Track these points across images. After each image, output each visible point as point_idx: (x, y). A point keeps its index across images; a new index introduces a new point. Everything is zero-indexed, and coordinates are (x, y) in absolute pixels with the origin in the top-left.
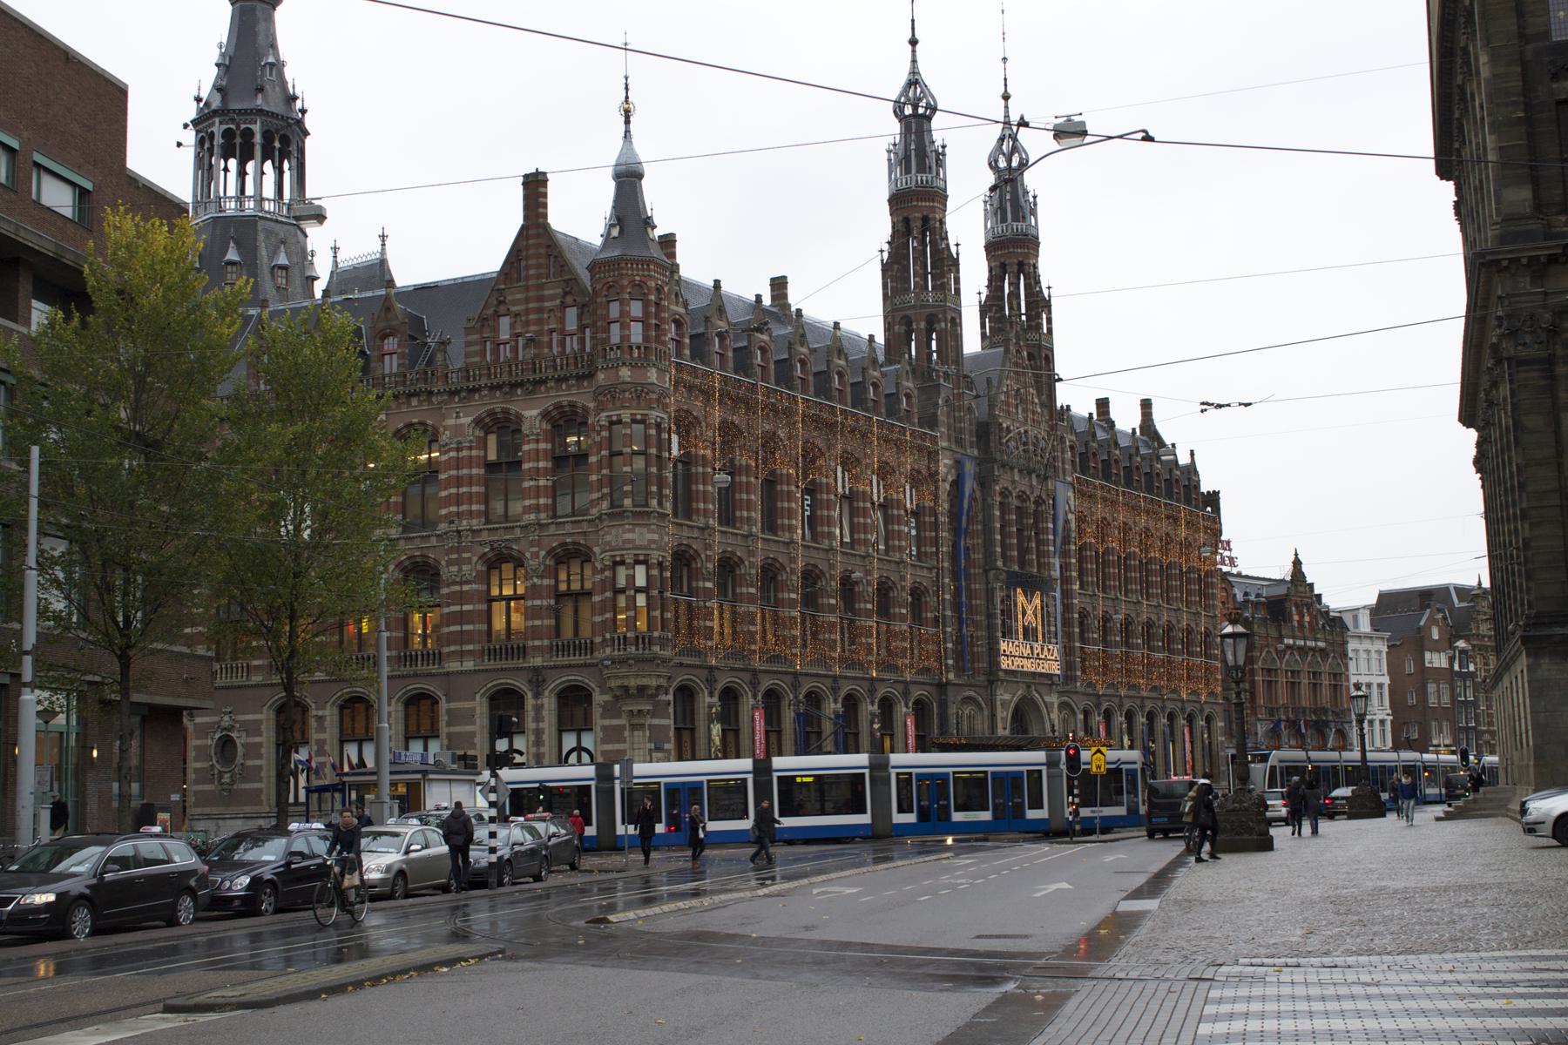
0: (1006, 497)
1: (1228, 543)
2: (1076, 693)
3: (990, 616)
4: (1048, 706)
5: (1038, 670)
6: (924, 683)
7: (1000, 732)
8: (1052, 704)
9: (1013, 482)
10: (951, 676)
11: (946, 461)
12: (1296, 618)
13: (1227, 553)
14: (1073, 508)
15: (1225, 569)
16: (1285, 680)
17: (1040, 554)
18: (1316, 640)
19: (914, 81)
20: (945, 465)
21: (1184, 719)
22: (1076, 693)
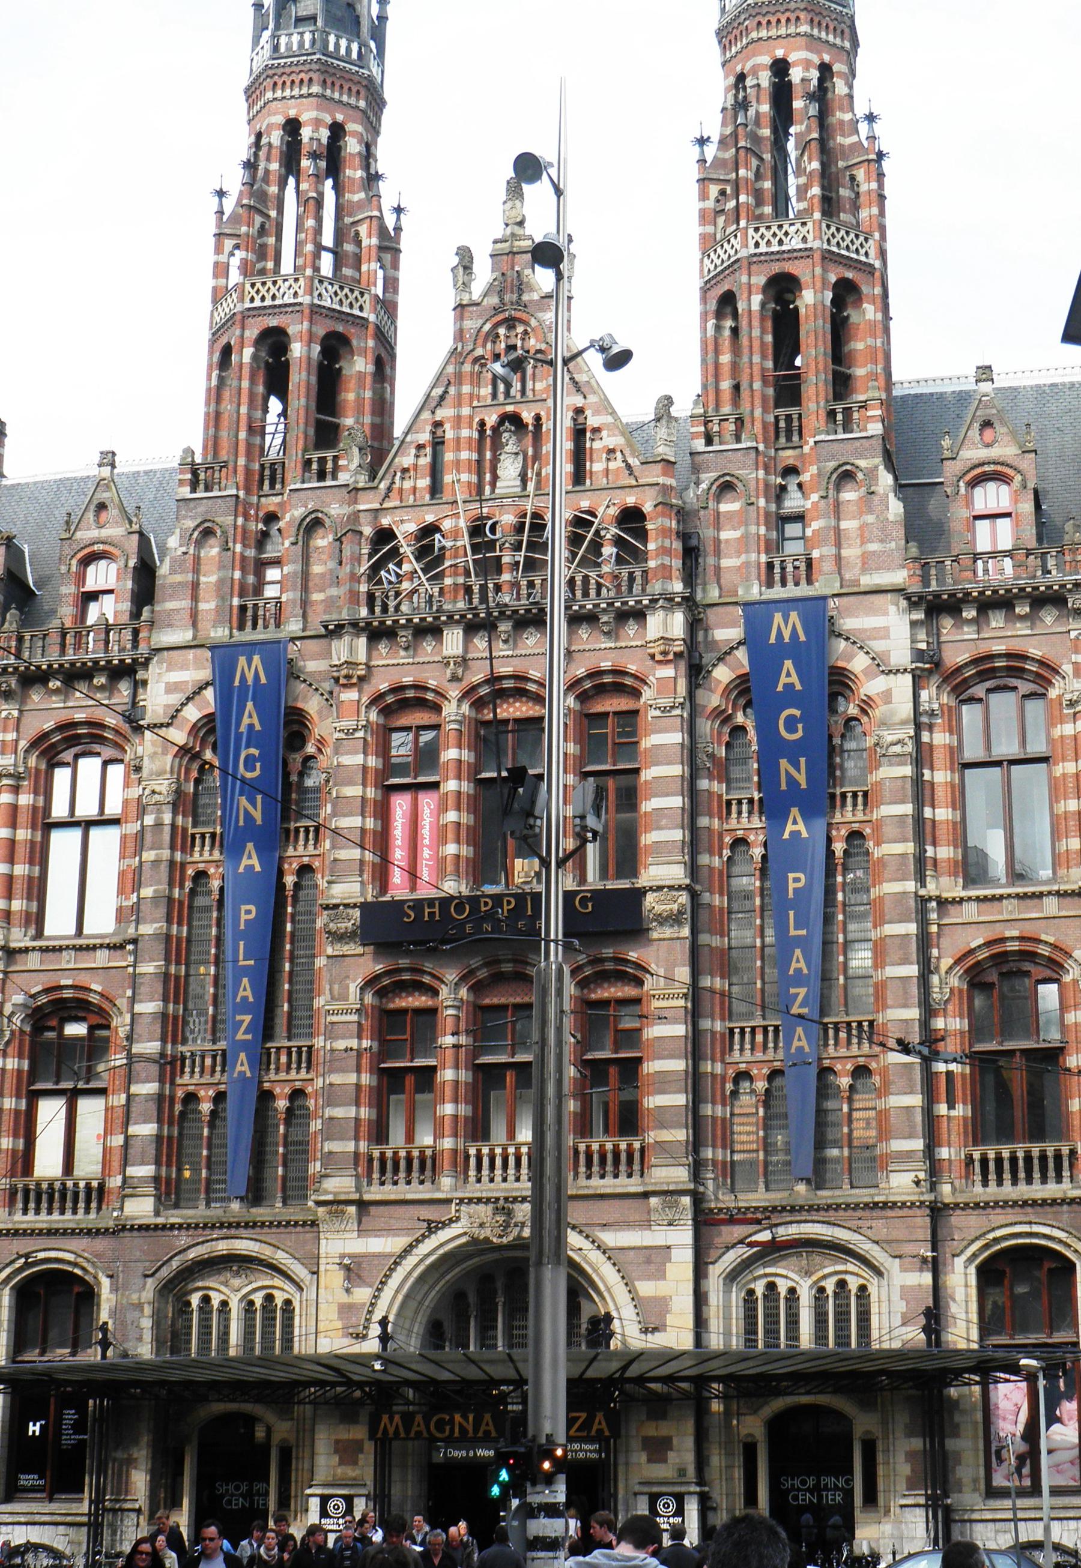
6: (51, 1233)
20: (171, 688)
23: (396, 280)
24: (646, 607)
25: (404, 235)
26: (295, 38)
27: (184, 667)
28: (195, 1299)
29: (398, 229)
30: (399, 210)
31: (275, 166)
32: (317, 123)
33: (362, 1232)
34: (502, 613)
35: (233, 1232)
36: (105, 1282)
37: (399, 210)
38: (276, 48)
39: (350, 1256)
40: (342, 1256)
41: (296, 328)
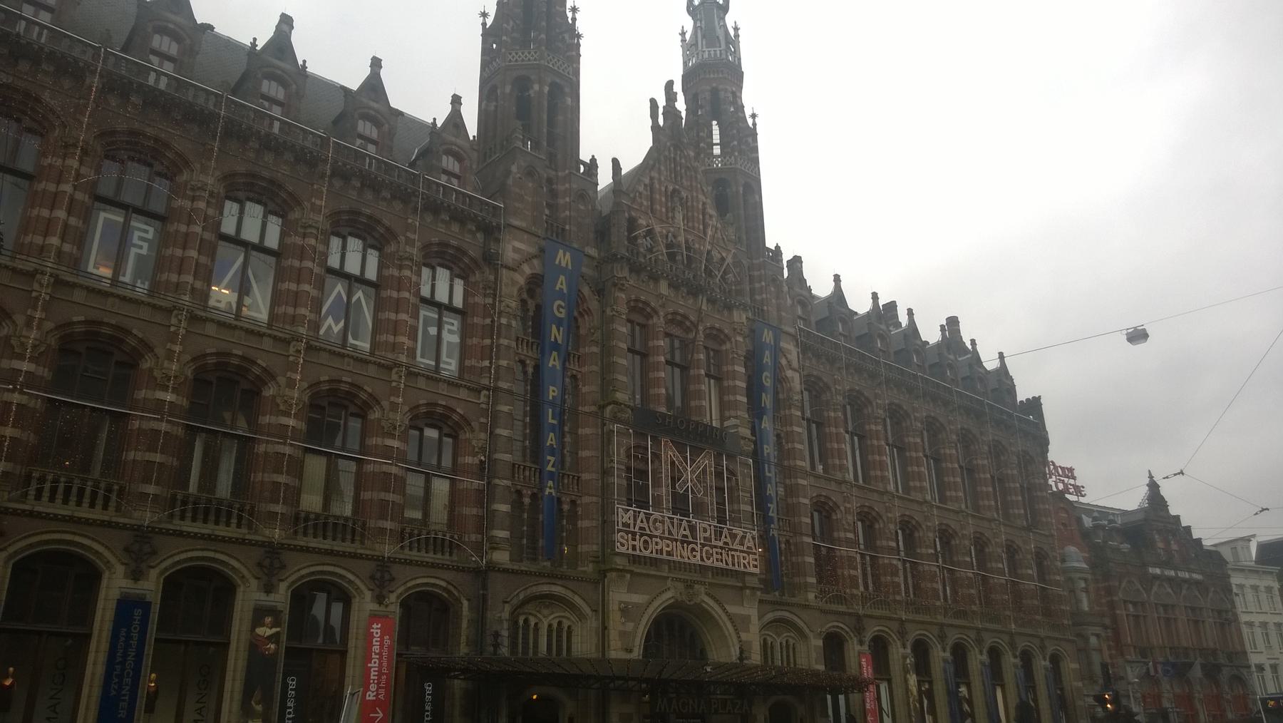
0: (649, 317)
1: (1071, 470)
2: (806, 607)
3: (606, 472)
4: (740, 623)
5: (708, 563)
6: (433, 566)
7: (615, 653)
8: (746, 620)
9: (660, 296)
10: (502, 557)
11: (517, 244)
12: (1160, 545)
13: (1072, 481)
14: (795, 364)
15: (1072, 498)
16: (1156, 615)
17: (723, 406)
18: (1190, 571)
20: (516, 250)
21: (1015, 657)
22: (806, 607)
24: (736, 306)
27: (521, 241)
28: (521, 622)
33: (629, 591)
34: (687, 284)
35: (553, 581)
36: (465, 603)
39: (624, 603)
40: (621, 602)
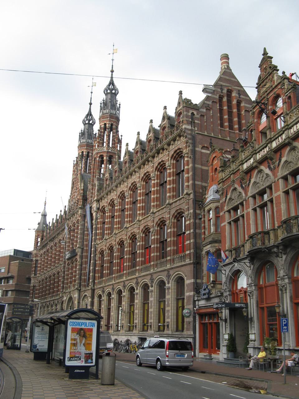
19: (112, 83)
23: (121, 147)
25: (122, 140)
26: (106, 111)
29: (121, 139)
30: (122, 136)
31: (103, 130)
32: (109, 124)
37: (122, 136)
38: (103, 113)
41: (105, 155)
